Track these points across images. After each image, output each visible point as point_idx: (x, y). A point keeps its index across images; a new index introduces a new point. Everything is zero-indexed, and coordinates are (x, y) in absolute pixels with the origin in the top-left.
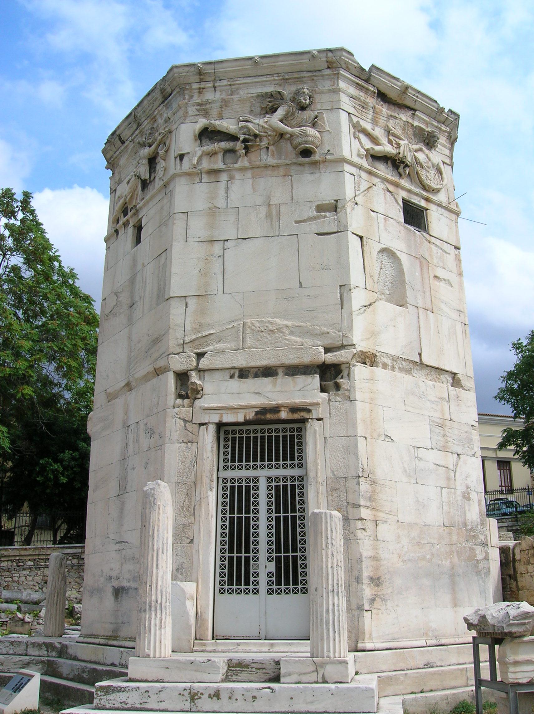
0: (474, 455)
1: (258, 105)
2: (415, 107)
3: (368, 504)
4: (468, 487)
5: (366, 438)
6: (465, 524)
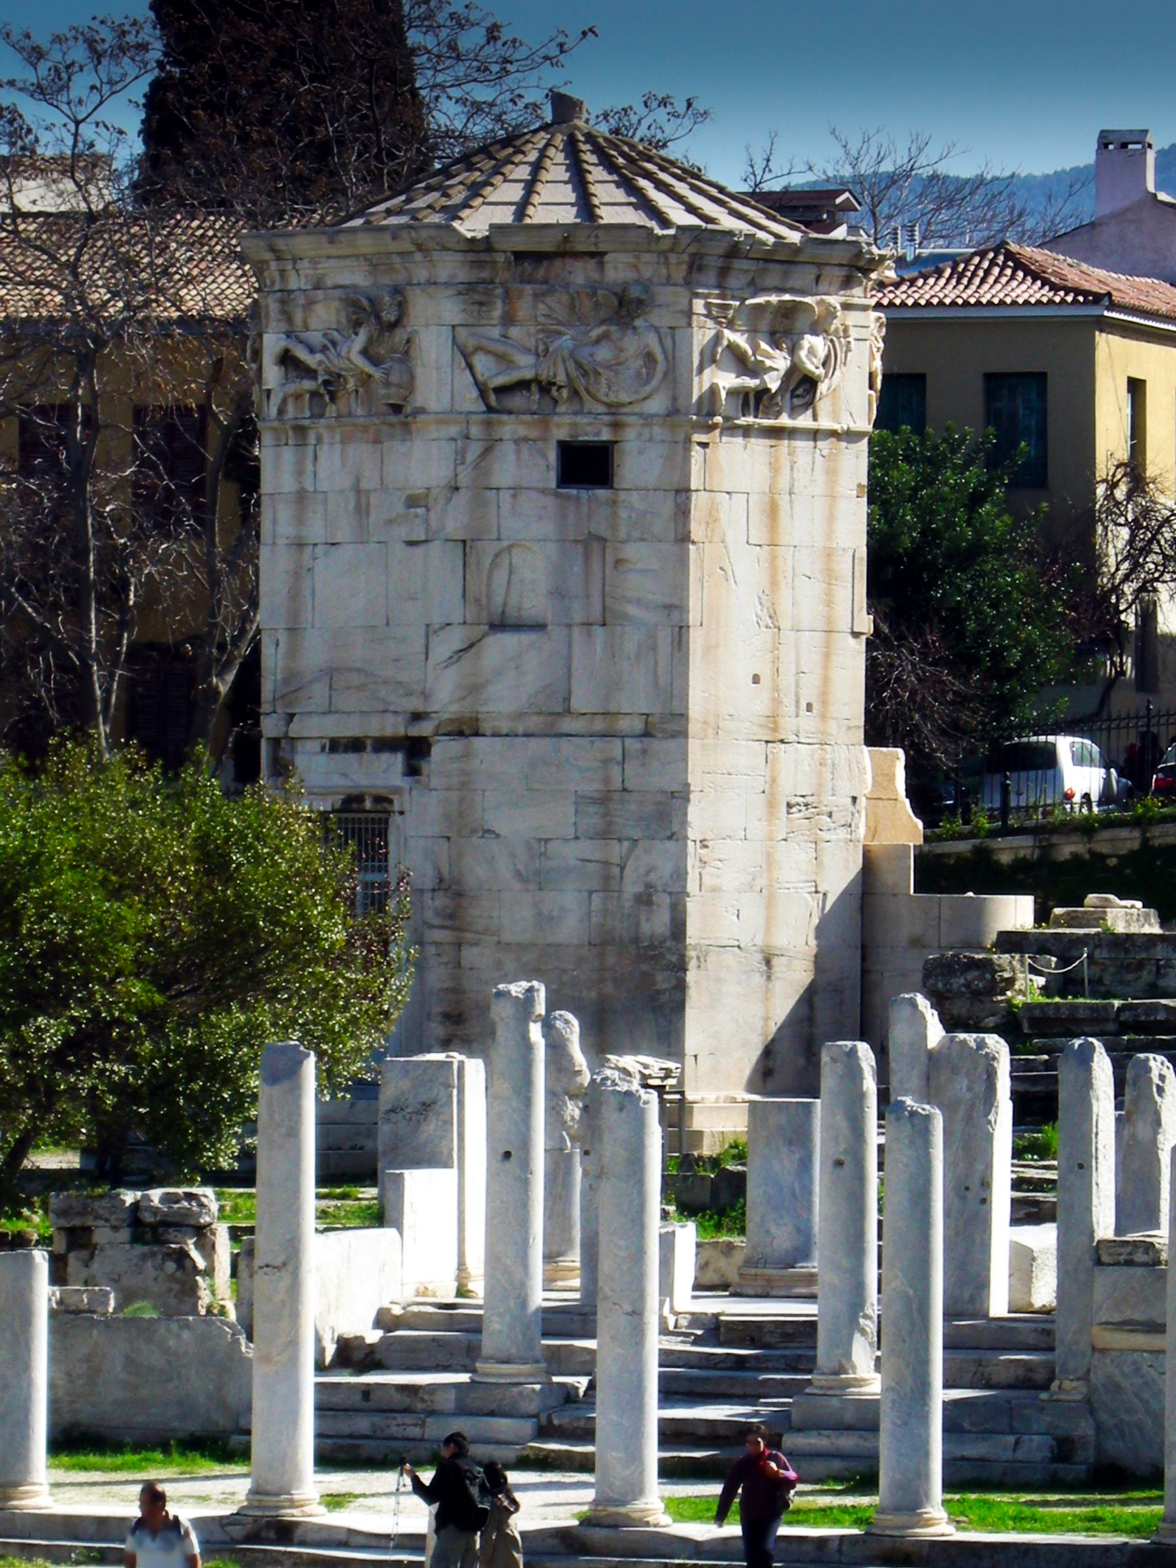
0: (670, 838)
1: (343, 314)
2: (602, 248)
3: (448, 923)
4: (649, 886)
5: (448, 838)
6: (636, 940)
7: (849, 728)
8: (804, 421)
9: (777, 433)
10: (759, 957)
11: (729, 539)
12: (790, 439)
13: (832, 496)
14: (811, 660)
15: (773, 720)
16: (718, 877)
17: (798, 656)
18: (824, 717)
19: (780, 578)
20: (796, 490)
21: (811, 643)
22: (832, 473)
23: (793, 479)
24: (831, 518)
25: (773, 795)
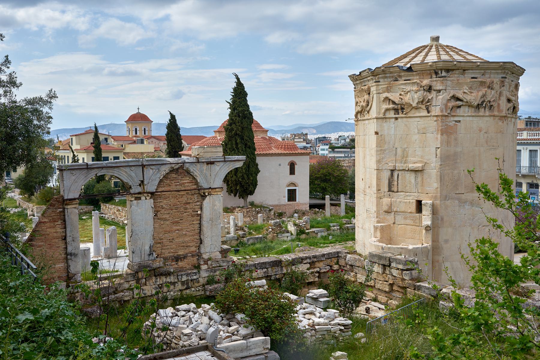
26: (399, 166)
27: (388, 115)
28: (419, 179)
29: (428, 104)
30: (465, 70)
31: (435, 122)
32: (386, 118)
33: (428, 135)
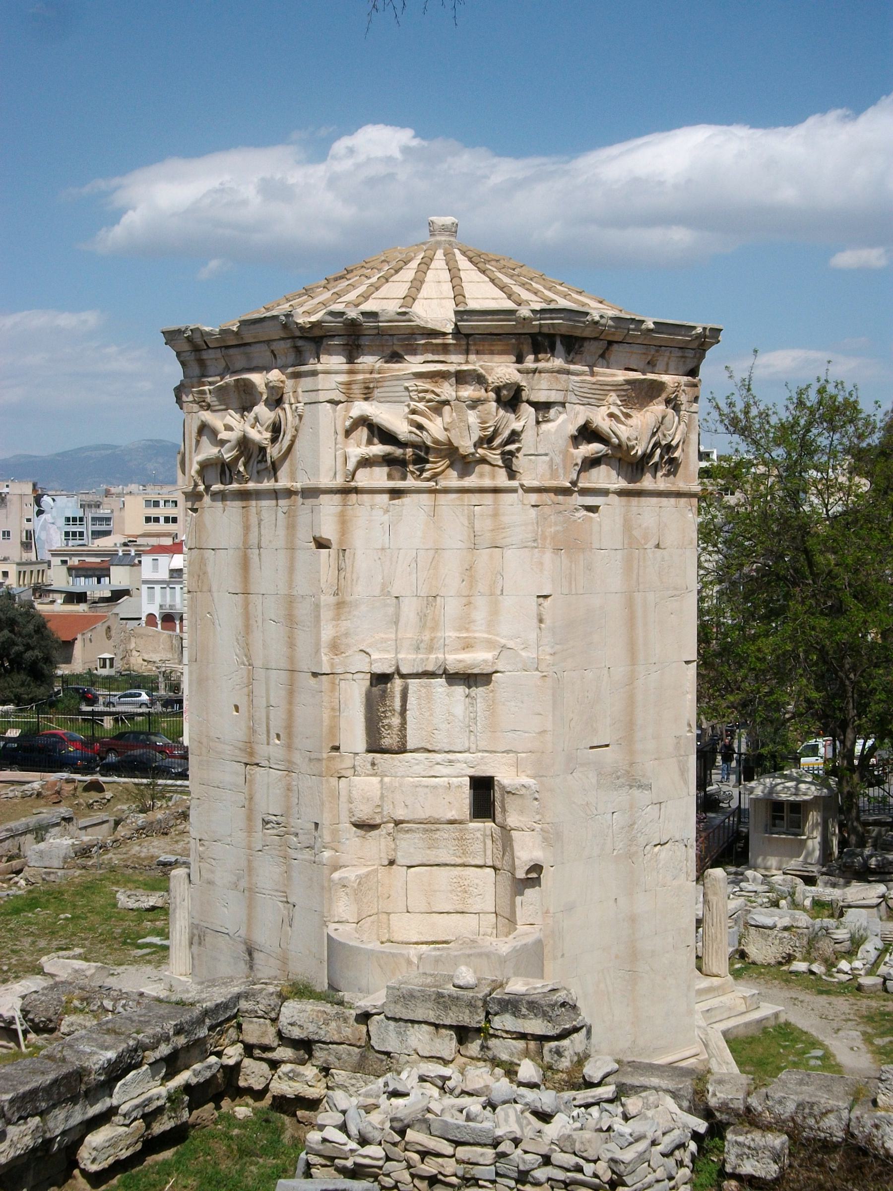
7: (310, 760)
8: (267, 484)
9: (245, 495)
10: (243, 947)
11: (214, 588)
12: (257, 499)
13: (291, 548)
14: (278, 696)
15: (249, 748)
16: (213, 872)
17: (267, 690)
18: (289, 747)
19: (252, 622)
20: (263, 545)
21: (278, 678)
22: (291, 527)
23: (260, 534)
24: (291, 570)
25: (251, 810)
26: (409, 662)
27: (364, 478)
28: (480, 705)
29: (508, 448)
30: (610, 343)
31: (533, 512)
32: (357, 491)
33: (510, 554)
